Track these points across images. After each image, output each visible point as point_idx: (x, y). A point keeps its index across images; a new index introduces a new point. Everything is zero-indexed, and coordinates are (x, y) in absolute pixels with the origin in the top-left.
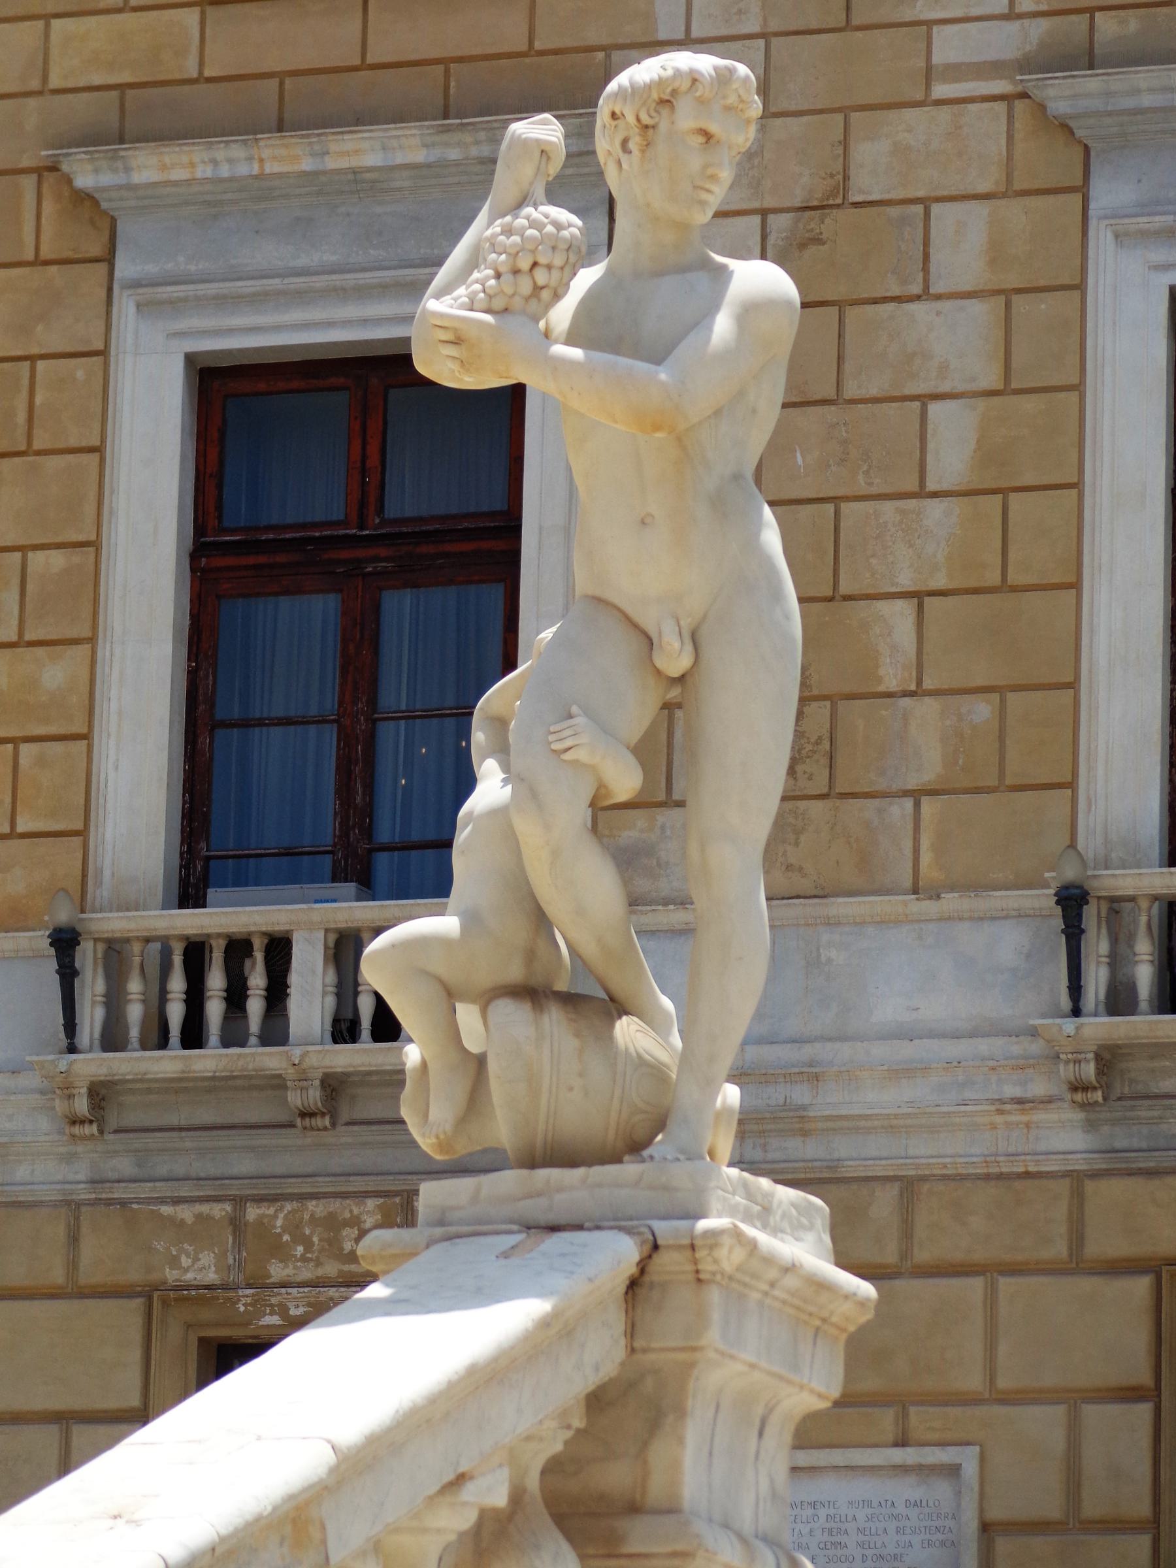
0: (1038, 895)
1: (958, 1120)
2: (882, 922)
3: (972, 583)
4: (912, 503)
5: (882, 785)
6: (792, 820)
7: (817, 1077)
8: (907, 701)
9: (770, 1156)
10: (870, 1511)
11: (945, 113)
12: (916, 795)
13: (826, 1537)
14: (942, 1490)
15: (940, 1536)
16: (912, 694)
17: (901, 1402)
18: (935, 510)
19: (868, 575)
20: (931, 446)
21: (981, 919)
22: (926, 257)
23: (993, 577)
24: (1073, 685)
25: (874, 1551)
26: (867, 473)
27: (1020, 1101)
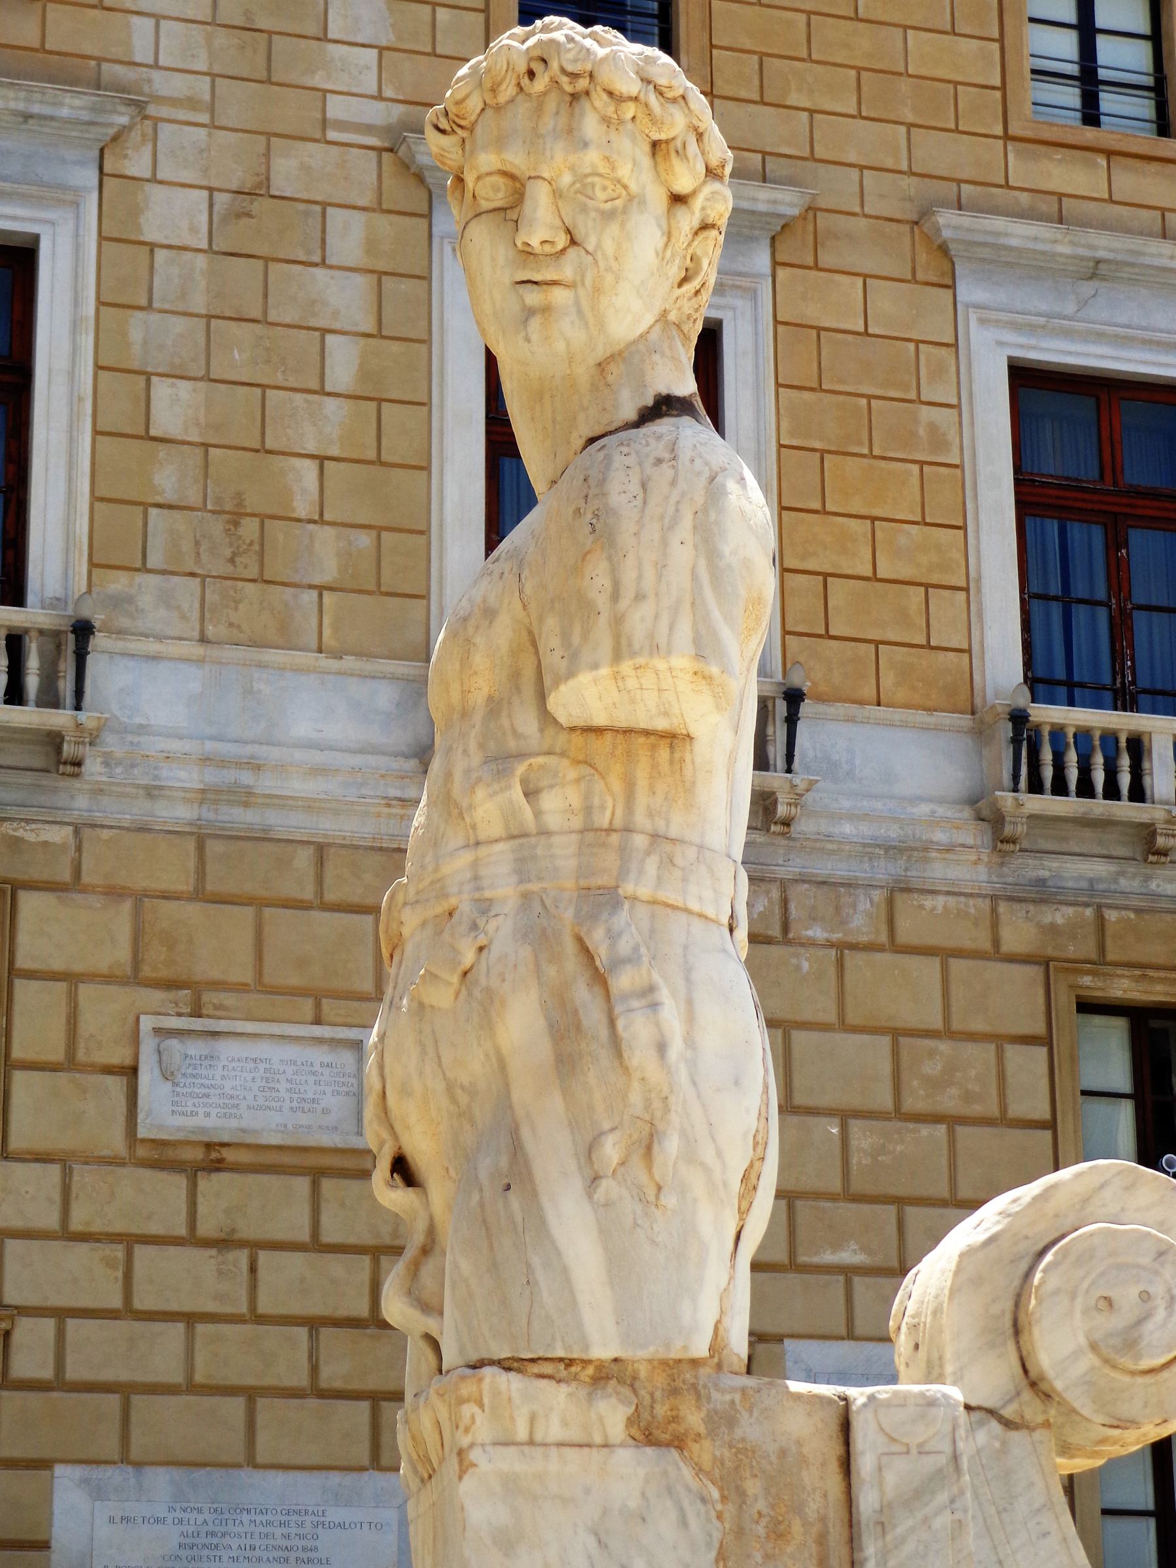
0: (409, 666)
1: (356, 807)
2: (298, 670)
3: (355, 456)
4: (316, 397)
5: (296, 578)
6: (232, 593)
7: (259, 768)
8: (311, 526)
9: (220, 818)
10: (295, 1068)
11: (334, 150)
12: (321, 589)
13: (264, 1084)
14: (347, 1058)
15: (345, 1089)
16: (315, 522)
17: (317, 996)
18: (331, 404)
19: (285, 439)
21: (366, 677)
22: (323, 241)
23: (371, 454)
25: (297, 1096)
26: (283, 372)
27: (400, 799)
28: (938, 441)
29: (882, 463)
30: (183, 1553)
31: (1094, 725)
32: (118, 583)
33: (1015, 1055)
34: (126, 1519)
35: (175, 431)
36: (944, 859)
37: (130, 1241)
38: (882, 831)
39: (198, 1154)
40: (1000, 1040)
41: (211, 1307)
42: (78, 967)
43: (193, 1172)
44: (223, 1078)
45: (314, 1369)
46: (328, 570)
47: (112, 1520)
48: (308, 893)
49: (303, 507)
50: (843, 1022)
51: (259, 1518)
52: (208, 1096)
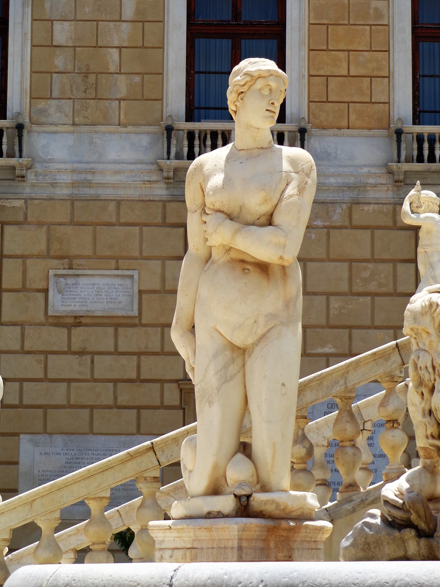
0: (154, 128)
1: (132, 185)
2: (110, 133)
3: (134, 45)
5: (110, 97)
6: (85, 105)
7: (94, 173)
9: (80, 193)
10: (108, 287)
12: (120, 100)
13: (96, 293)
14: (128, 282)
15: (128, 294)
16: (118, 73)
17: (117, 259)
18: (124, 25)
19: (106, 41)
20: (123, 8)
21: (137, 133)
23: (140, 44)
24: (162, 74)
25: (109, 297)
26: (105, 14)
27: (149, 181)
28: (378, 14)
29: (354, 27)
30: (67, 465)
31: (435, 132)
32: (41, 104)
33: (401, 267)
34: (46, 454)
35: (63, 43)
36: (374, 190)
37: (46, 353)
38: (347, 180)
39: (72, 320)
40: (394, 261)
41: (77, 376)
42: (27, 253)
43: (69, 327)
44: (81, 291)
45: (116, 398)
46: (123, 92)
47: (41, 454)
48: (113, 220)
49: (113, 68)
50: (329, 257)
51: (95, 453)
52: (75, 299)
